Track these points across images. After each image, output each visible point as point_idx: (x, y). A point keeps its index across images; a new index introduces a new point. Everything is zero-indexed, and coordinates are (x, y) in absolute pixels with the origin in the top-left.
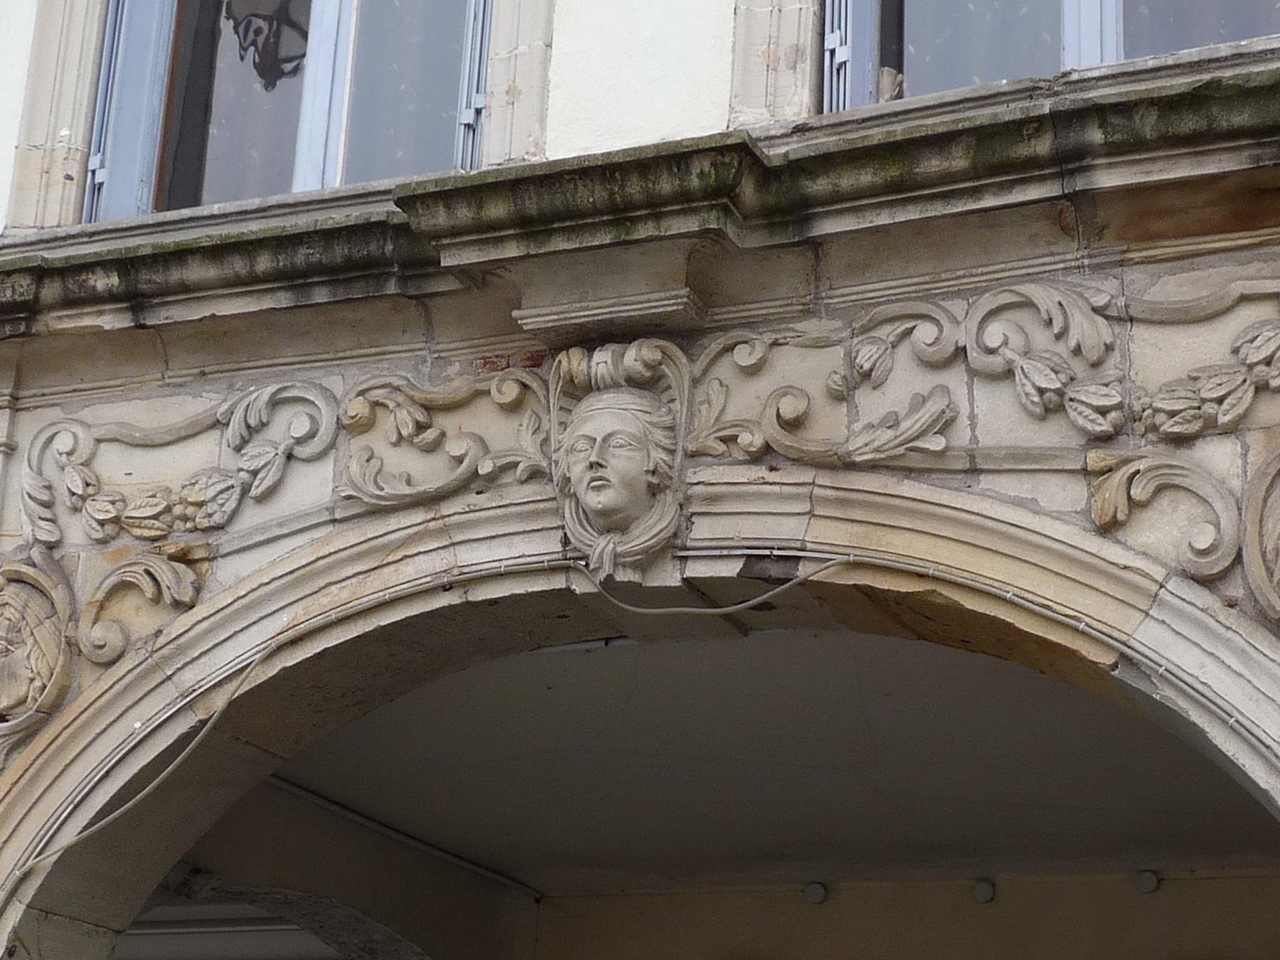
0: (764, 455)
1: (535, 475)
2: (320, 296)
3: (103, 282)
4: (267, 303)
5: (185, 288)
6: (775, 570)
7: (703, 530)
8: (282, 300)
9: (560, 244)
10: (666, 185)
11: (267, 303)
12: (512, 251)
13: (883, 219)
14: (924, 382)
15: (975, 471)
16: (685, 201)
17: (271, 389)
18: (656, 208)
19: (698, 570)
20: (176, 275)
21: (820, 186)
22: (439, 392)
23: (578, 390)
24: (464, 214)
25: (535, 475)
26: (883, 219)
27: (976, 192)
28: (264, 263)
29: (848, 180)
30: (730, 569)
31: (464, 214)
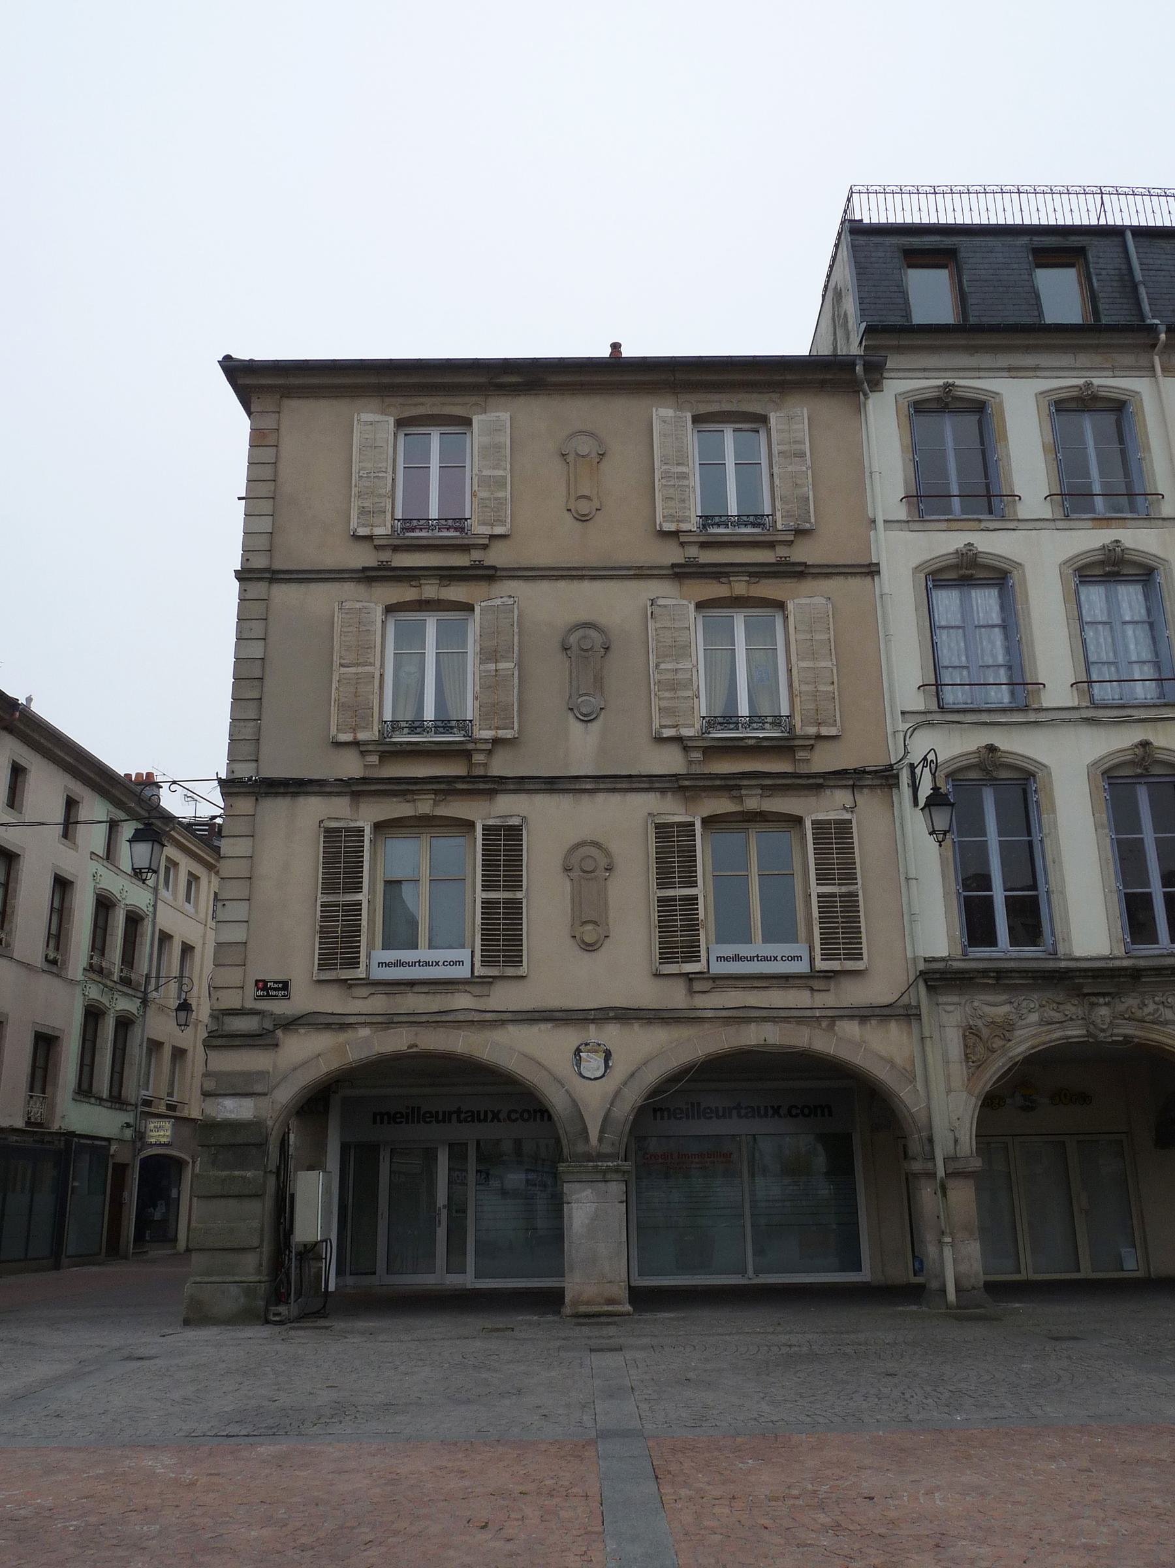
0: (1129, 1019)
1: (1082, 1018)
2: (1040, 981)
3: (992, 974)
4: (1027, 982)
5: (1011, 977)
6: (1130, 1039)
7: (1115, 1031)
8: (1031, 982)
9: (1100, 980)
10: (1123, 973)
11: (1027, 982)
12: (1090, 981)
13: (1154, 979)
14: (1155, 1007)
15: (1166, 1024)
16: (1125, 976)
17: (1023, 997)
18: (1119, 976)
19: (1114, 1038)
20: (1009, 975)
21: (1144, 973)
22: (1058, 1000)
23: (1093, 1005)
24: (1082, 974)
25: (1082, 1018)
26: (1154, 979)
27: (1170, 977)
28: (1030, 975)
29: (1149, 973)
30: (1121, 1039)
31: (1082, 974)
